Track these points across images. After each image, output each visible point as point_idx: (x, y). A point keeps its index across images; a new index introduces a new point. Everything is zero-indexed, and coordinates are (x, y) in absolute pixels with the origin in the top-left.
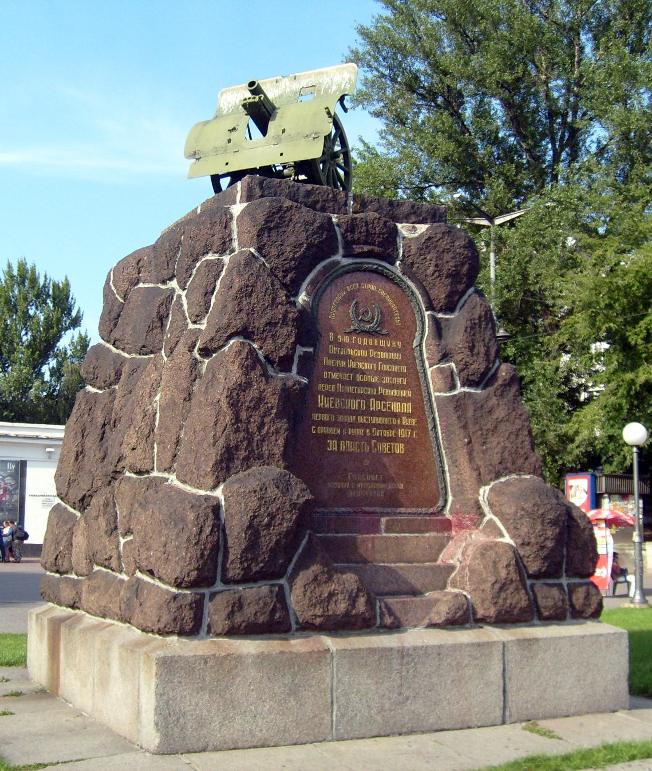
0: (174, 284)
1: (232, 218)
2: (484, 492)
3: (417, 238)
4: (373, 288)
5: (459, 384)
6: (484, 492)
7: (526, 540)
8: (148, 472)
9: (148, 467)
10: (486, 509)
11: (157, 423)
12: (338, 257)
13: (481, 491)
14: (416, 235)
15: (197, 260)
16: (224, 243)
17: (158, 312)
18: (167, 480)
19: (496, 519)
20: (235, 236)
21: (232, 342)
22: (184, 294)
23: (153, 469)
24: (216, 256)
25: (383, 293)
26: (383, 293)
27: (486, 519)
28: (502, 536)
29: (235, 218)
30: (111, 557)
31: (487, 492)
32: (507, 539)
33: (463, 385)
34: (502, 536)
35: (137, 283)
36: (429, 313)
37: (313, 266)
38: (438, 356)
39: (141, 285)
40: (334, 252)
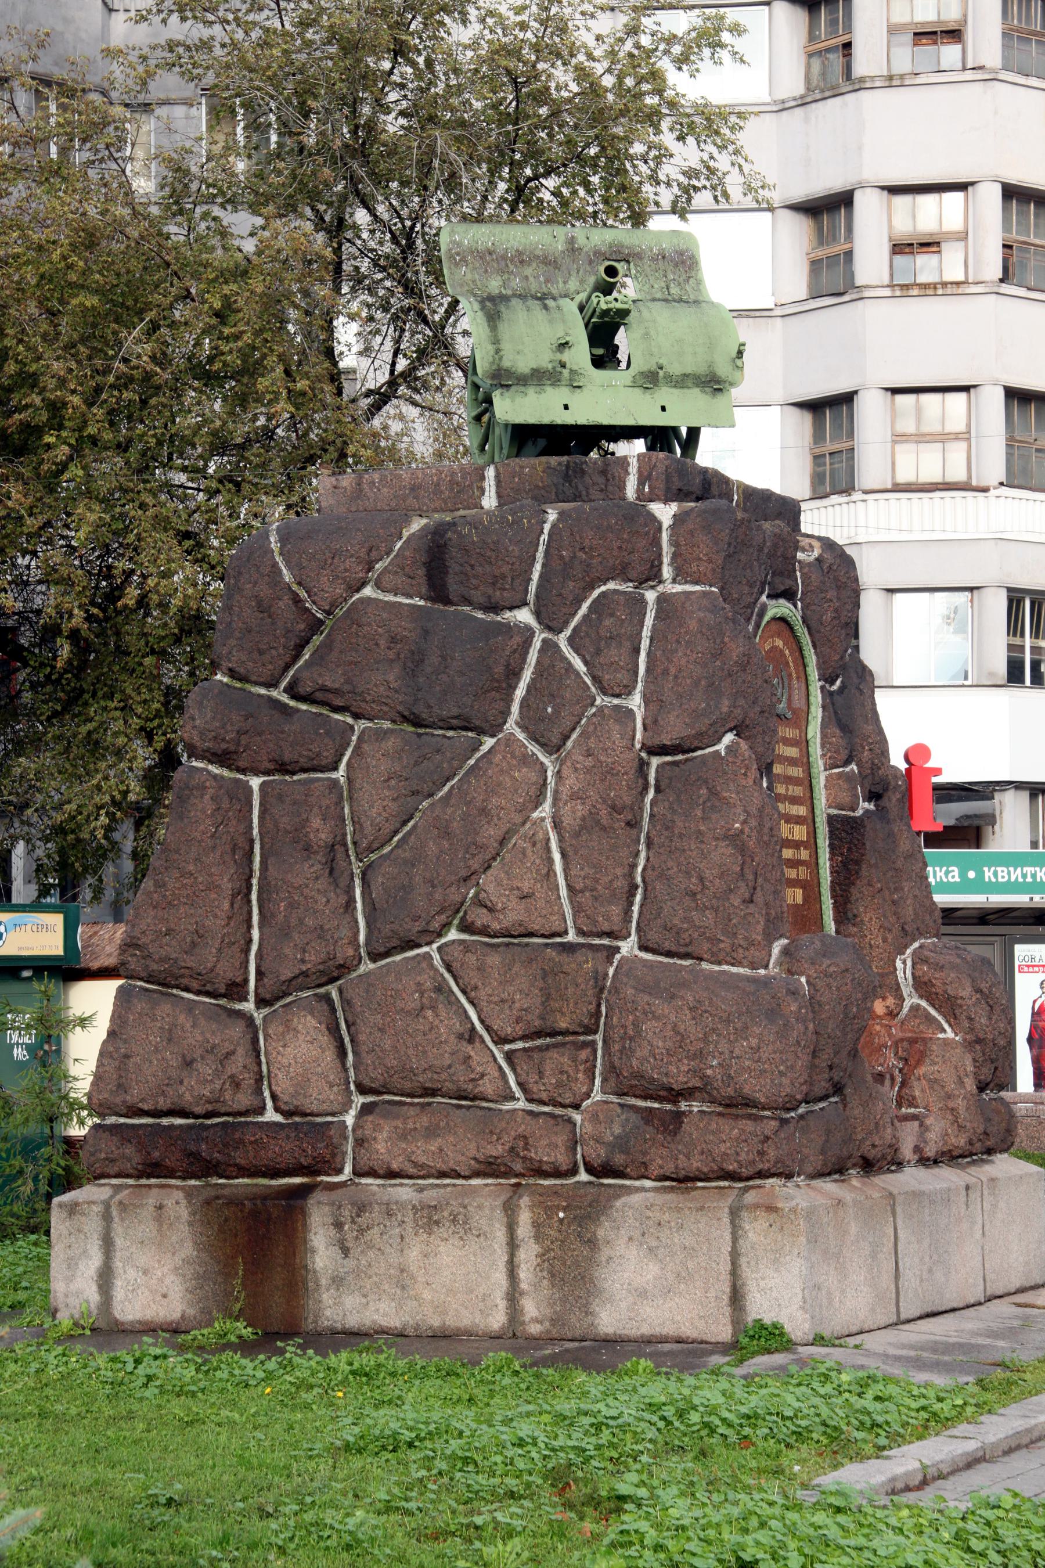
0: (524, 616)
4: (780, 643)
6: (904, 962)
7: (981, 1035)
10: (906, 990)
12: (764, 598)
13: (899, 964)
16: (652, 566)
17: (508, 665)
18: (617, 949)
19: (924, 1003)
20: (666, 560)
21: (729, 738)
22: (562, 640)
23: (566, 932)
24: (628, 587)
25: (787, 653)
26: (787, 653)
28: (944, 1031)
31: (909, 963)
32: (950, 1034)
35: (358, 590)
38: (844, 755)
39: (368, 591)
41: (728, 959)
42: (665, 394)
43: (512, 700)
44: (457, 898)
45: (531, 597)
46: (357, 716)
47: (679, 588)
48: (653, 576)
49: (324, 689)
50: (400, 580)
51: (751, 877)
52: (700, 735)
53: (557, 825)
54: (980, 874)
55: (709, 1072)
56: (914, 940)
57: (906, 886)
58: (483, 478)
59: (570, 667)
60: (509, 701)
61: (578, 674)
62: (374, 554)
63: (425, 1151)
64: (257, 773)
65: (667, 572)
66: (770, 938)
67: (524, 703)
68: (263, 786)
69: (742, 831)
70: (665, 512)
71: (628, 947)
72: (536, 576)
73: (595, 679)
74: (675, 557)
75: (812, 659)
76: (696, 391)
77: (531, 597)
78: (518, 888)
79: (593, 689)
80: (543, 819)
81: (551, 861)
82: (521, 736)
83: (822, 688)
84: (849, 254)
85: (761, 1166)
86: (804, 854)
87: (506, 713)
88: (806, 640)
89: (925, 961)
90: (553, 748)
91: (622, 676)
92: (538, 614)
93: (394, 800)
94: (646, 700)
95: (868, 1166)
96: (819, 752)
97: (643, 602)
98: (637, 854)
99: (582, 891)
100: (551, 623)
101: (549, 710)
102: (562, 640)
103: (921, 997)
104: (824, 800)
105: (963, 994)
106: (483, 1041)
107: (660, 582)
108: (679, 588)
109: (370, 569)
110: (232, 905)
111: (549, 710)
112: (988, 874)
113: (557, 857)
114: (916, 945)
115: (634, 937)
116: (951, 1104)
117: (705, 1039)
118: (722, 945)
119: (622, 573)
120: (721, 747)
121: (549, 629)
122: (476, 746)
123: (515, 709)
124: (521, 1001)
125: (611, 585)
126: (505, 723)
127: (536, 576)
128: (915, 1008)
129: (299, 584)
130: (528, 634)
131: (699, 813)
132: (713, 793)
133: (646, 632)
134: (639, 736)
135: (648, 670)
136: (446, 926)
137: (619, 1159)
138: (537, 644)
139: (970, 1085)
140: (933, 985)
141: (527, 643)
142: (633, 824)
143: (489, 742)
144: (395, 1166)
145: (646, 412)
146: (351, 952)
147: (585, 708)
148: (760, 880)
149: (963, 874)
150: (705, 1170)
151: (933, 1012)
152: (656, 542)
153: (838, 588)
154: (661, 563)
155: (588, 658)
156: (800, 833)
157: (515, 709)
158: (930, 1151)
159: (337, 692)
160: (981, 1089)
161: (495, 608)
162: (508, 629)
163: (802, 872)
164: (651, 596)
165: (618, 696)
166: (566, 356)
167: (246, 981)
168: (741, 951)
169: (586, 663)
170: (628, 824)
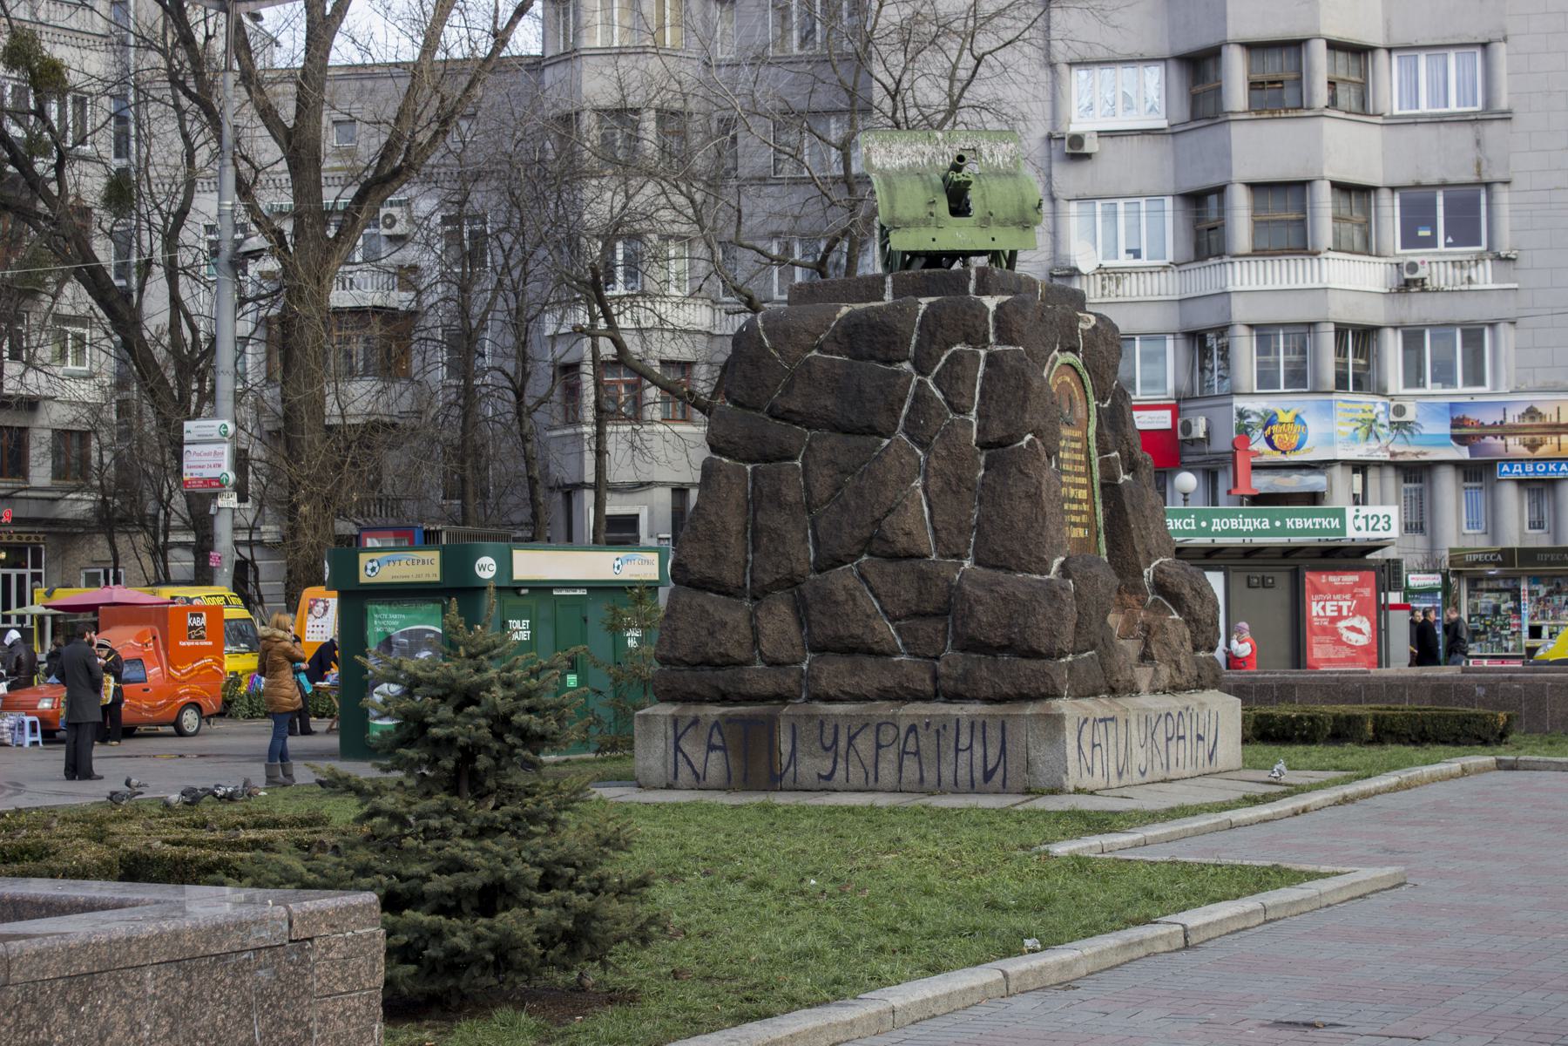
0: (907, 366)
12: (1056, 352)
15: (948, 346)
21: (1029, 437)
22: (929, 381)
27: (1150, 599)
32: (1176, 616)
39: (815, 353)
42: (995, 231)
47: (999, 348)
48: (985, 342)
50: (834, 347)
53: (925, 491)
54: (1284, 524)
57: (1151, 526)
58: (884, 282)
59: (933, 397)
60: (897, 417)
63: (849, 683)
64: (750, 461)
65: (992, 339)
67: (907, 418)
68: (754, 469)
71: (967, 564)
73: (949, 403)
84: (1220, 88)
86: (1085, 507)
87: (896, 425)
88: (1086, 376)
89: (1162, 571)
92: (914, 364)
94: (980, 415)
95: (1113, 691)
97: (978, 356)
102: (929, 381)
108: (999, 348)
112: (1289, 523)
113: (926, 509)
117: (1011, 617)
119: (967, 340)
120: (1024, 443)
121: (921, 373)
122: (879, 443)
123: (901, 421)
125: (959, 347)
128: (1155, 601)
135: (982, 397)
137: (961, 687)
139: (1188, 646)
143: (886, 442)
144: (832, 693)
145: (980, 240)
149: (1272, 523)
156: (1082, 494)
157: (901, 421)
159: (798, 413)
160: (1196, 648)
161: (889, 362)
162: (898, 374)
163: (1084, 518)
164: (982, 353)
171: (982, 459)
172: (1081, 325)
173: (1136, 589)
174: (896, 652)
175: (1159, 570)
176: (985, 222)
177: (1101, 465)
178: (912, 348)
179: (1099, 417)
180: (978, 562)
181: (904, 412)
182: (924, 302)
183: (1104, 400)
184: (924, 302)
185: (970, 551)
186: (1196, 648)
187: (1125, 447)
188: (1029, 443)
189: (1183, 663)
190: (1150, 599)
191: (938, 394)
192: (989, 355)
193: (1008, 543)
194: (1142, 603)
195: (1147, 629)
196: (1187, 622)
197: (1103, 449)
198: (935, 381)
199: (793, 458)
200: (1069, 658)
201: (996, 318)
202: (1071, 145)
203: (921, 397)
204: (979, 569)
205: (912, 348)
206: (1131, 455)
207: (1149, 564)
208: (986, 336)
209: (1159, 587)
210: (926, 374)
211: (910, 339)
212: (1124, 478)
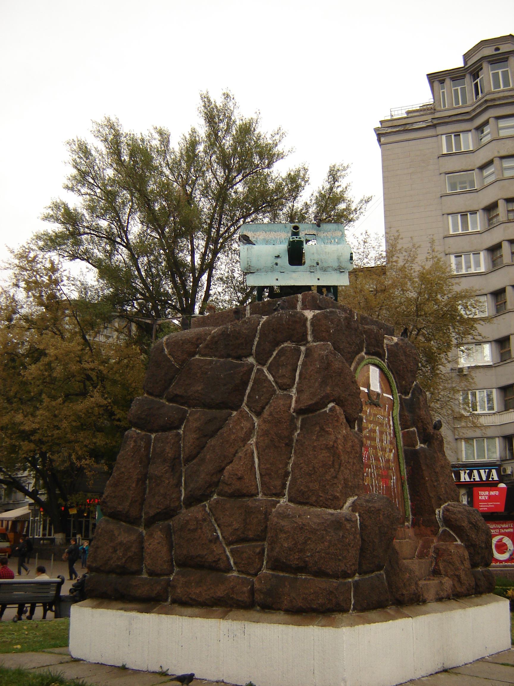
0: (251, 360)
1: (307, 319)
2: (439, 512)
3: (392, 345)
5: (419, 443)
6: (439, 512)
8: (252, 495)
9: (253, 492)
11: (256, 460)
13: (437, 511)
14: (393, 343)
15: (278, 345)
16: (303, 335)
18: (279, 502)
19: (447, 529)
20: (309, 332)
21: (331, 405)
23: (258, 494)
24: (293, 345)
27: (441, 530)
28: (457, 541)
29: (309, 319)
30: (219, 559)
31: (441, 512)
32: (459, 542)
33: (421, 443)
34: (457, 541)
35: (194, 356)
36: (399, 394)
37: (354, 359)
39: (197, 357)
40: (362, 351)
41: (324, 505)
43: (245, 395)
44: (216, 480)
45: (254, 351)
46: (189, 407)
48: (303, 339)
49: (177, 395)
51: (337, 467)
52: (316, 404)
55: (307, 559)
56: (446, 502)
57: (441, 479)
59: (266, 379)
61: (270, 381)
62: (199, 341)
65: (310, 338)
66: (347, 496)
69: (333, 446)
70: (309, 314)
71: (283, 501)
72: (256, 343)
73: (276, 383)
74: (313, 331)
75: (394, 385)
76: (333, 272)
77: (254, 351)
78: (237, 475)
79: (276, 387)
80: (251, 444)
81: (253, 462)
82: (247, 410)
83: (400, 397)
84: (510, 350)
85: (329, 606)
90: (258, 414)
91: (286, 381)
93: (198, 439)
96: (399, 422)
97: (299, 351)
98: (290, 458)
99: (265, 475)
100: (262, 361)
101: (257, 397)
103: (447, 526)
104: (402, 443)
105: (463, 525)
106: (221, 543)
107: (309, 342)
109: (198, 346)
110: (137, 485)
111: (257, 397)
113: (256, 460)
114: (446, 504)
115: (286, 496)
116: (457, 573)
117: (305, 543)
118: (321, 499)
119: (289, 338)
120: (327, 409)
121: (260, 364)
123: (246, 398)
124: (236, 525)
125: (286, 344)
126: (242, 405)
127: (256, 343)
128: (444, 531)
129: (170, 354)
130: (253, 366)
131: (314, 438)
132: (322, 429)
133: (300, 363)
134: (293, 405)
135: (300, 379)
136: (212, 493)
138: (255, 370)
139: (467, 564)
140: (451, 521)
141: (251, 370)
142: (289, 445)
143: (235, 413)
146: (177, 504)
147: (272, 395)
148: (342, 468)
150: (304, 607)
151: (452, 533)
152: (305, 325)
153: (405, 356)
154: (307, 334)
155: (274, 374)
158: (444, 594)
164: (303, 348)
165: (286, 390)
166: (278, 261)
167: (141, 517)
168: (329, 501)
169: (273, 376)
170: (287, 444)
171: (299, 424)
172: (385, 341)
173: (432, 524)
174: (229, 569)
175: (446, 510)
176: (312, 270)
177: (403, 437)
178: (254, 348)
179: (401, 404)
180: (290, 500)
181: (248, 391)
182: (265, 318)
183: (406, 394)
184: (265, 318)
185: (286, 492)
186: (474, 565)
187: (420, 425)
188: (331, 410)
189: (463, 576)
190: (441, 530)
191: (270, 377)
192: (307, 349)
193: (311, 485)
194: (435, 533)
195: (437, 551)
196: (467, 547)
197: (404, 426)
198: (269, 369)
199: (179, 427)
200: (357, 577)
201: (312, 324)
202: (459, 372)
203: (261, 380)
204: (292, 505)
205: (254, 348)
206: (425, 430)
207: (439, 506)
208: (305, 335)
209: (447, 521)
210: (263, 365)
211: (253, 341)
212: (419, 446)
